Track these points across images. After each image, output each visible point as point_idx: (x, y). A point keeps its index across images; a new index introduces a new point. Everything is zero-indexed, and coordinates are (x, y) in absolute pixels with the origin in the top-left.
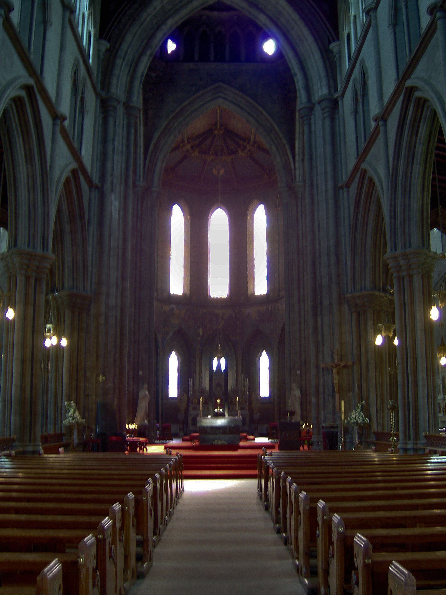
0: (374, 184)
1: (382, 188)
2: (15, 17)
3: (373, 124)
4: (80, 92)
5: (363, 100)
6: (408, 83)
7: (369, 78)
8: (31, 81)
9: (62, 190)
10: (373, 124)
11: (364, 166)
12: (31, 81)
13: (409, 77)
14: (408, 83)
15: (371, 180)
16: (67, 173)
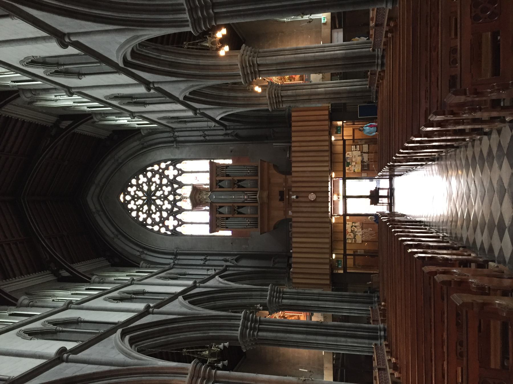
0: (194, 91)
1: (198, 85)
2: (70, 345)
3: (152, 91)
4: (129, 296)
5: (135, 98)
6: (121, 65)
7: (119, 93)
8: (119, 331)
9: (199, 307)
10: (152, 91)
11: (181, 98)
12: (119, 331)
13: (117, 64)
14: (121, 65)
15: (190, 93)
16: (186, 303)
